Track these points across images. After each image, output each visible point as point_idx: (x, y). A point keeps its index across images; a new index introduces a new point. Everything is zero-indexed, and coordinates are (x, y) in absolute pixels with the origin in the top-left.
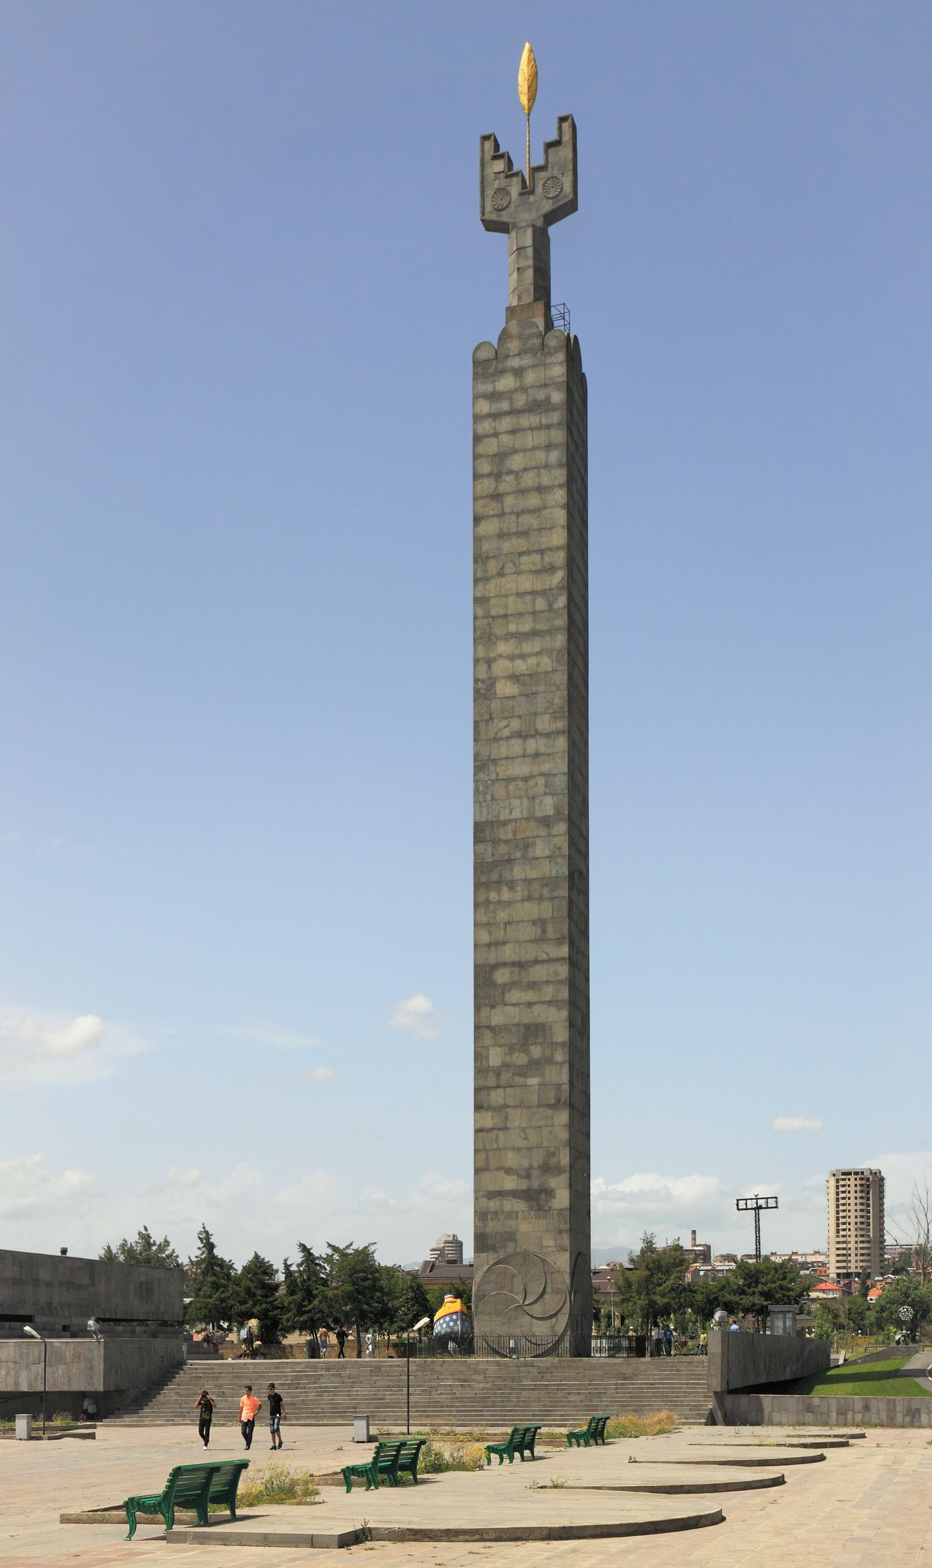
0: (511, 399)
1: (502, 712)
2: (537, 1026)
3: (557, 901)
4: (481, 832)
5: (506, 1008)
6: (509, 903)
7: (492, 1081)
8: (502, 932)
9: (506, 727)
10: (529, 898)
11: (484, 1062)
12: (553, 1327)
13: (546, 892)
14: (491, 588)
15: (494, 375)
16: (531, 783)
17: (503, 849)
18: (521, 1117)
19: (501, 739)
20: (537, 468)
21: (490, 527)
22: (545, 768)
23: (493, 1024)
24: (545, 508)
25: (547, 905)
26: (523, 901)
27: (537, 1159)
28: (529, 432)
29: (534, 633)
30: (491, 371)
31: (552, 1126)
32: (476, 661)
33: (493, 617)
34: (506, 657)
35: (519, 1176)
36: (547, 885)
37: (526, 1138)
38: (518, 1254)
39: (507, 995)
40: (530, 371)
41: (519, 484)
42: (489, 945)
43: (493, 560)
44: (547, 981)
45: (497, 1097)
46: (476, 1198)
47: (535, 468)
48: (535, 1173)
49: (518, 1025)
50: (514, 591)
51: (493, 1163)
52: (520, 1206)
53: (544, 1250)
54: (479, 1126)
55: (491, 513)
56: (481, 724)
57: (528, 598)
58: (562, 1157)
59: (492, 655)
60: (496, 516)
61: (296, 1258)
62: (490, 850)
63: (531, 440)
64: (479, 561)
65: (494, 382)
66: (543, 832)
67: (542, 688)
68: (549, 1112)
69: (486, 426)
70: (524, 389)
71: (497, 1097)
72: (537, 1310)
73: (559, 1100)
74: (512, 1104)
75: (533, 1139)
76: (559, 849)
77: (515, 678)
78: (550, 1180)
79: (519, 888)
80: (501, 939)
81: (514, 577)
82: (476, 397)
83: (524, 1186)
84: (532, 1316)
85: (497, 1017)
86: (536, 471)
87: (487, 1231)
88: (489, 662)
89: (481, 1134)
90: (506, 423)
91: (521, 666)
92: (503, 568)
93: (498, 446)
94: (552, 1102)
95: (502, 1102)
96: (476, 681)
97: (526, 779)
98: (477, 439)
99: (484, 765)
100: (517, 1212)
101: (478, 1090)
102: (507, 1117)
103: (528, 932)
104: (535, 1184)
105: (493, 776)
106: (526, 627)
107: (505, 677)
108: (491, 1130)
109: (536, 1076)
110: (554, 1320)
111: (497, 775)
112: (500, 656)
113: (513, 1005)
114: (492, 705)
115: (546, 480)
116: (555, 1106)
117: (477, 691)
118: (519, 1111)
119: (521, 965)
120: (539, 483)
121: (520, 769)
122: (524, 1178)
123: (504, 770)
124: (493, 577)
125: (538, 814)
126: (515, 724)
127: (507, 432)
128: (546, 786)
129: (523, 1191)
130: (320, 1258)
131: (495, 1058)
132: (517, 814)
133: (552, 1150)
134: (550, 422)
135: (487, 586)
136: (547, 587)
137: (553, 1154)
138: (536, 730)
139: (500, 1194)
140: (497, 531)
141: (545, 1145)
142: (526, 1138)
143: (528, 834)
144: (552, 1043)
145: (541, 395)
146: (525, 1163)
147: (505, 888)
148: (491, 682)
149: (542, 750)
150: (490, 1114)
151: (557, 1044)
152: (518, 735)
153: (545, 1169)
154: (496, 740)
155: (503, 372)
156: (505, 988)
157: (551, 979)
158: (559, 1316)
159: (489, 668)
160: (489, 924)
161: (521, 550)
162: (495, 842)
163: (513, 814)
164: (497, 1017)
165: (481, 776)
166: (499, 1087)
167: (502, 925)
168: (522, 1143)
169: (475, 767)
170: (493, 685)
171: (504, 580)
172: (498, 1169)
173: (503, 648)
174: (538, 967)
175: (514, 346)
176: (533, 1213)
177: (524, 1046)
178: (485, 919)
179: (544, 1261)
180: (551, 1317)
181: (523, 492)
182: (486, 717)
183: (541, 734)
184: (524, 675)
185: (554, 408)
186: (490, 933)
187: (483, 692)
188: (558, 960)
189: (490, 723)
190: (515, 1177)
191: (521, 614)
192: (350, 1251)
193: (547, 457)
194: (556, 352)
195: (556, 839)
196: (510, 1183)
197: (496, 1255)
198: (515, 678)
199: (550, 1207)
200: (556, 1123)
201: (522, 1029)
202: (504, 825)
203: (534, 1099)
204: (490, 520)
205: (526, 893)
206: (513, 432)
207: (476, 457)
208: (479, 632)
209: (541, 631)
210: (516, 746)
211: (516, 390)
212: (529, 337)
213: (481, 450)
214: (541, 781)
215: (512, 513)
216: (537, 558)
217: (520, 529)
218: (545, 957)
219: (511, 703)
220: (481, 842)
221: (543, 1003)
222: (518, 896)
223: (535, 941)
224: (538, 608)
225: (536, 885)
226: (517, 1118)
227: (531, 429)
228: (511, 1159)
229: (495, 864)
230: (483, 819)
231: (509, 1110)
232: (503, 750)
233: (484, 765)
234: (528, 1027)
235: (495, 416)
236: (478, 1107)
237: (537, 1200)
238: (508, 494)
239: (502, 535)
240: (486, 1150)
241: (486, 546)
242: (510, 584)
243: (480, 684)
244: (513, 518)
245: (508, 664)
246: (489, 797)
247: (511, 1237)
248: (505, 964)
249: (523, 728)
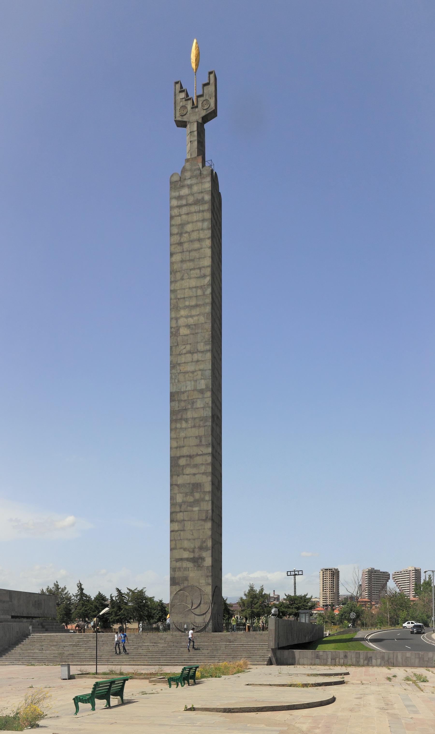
0: (187, 199)
1: (182, 342)
2: (197, 484)
3: (206, 428)
4: (173, 396)
5: (184, 476)
6: (186, 429)
7: (178, 509)
8: (182, 442)
9: (184, 349)
10: (194, 426)
11: (175, 501)
12: (204, 619)
13: (201, 423)
14: (178, 285)
15: (179, 188)
16: (195, 374)
17: (183, 404)
19: (182, 354)
20: (198, 230)
21: (177, 258)
22: (202, 367)
23: (178, 483)
24: (201, 248)
25: (202, 429)
26: (191, 427)
27: (197, 544)
28: (195, 214)
29: (197, 306)
30: (178, 186)
31: (204, 529)
32: (171, 319)
33: (179, 299)
34: (184, 317)
35: (190, 552)
36: (202, 420)
37: (193, 535)
38: (188, 586)
39: (184, 470)
40: (195, 186)
41: (190, 238)
42: (176, 448)
43: (178, 273)
44: (202, 464)
45: (180, 516)
46: (171, 562)
47: (197, 230)
48: (197, 550)
49: (189, 484)
50: (188, 287)
51: (178, 546)
52: (190, 565)
54: (172, 529)
55: (178, 251)
56: (173, 347)
57: (194, 290)
58: (208, 543)
59: (178, 316)
60: (180, 253)
61: (115, 594)
62: (177, 405)
63: (195, 217)
64: (173, 273)
65: (179, 191)
66: (200, 396)
67: (200, 331)
68: (203, 523)
69: (176, 212)
70: (192, 194)
71: (180, 516)
72: (197, 611)
73: (207, 517)
74: (186, 519)
76: (208, 404)
77: (188, 326)
79: (190, 422)
80: (182, 445)
81: (188, 280)
82: (171, 199)
83: (191, 556)
84: (195, 614)
85: (180, 480)
86: (198, 232)
88: (177, 319)
89: (173, 533)
90: (184, 210)
91: (191, 321)
92: (183, 276)
93: (181, 221)
94: (204, 518)
95: (182, 518)
96: (171, 328)
97: (193, 372)
98: (172, 218)
99: (175, 366)
100: (189, 568)
101: (171, 513)
102: (184, 526)
103: (194, 442)
104: (197, 555)
105: (179, 371)
106: (193, 303)
107: (183, 326)
109: (197, 507)
110: (205, 616)
111: (181, 370)
112: (182, 316)
113: (187, 475)
114: (178, 339)
115: (202, 236)
116: (205, 520)
117: (171, 333)
118: (189, 523)
119: (190, 457)
120: (199, 237)
121: (190, 368)
122: (192, 552)
123: (183, 368)
124: (178, 281)
125: (198, 388)
126: (188, 347)
127: (185, 214)
128: (202, 375)
129: (191, 558)
130: (124, 594)
131: (179, 499)
132: (189, 388)
133: (204, 540)
134: (204, 209)
135: (176, 285)
136: (202, 284)
137: (204, 542)
138: (197, 350)
139: (181, 560)
140: (181, 259)
141: (201, 537)
142: (193, 535)
143: (194, 397)
144: (204, 492)
145: (200, 197)
146: (192, 546)
147: (184, 422)
148: (178, 328)
149: (200, 358)
150: (177, 524)
151: (207, 492)
152: (190, 352)
153: (201, 548)
154: (180, 354)
155: (183, 187)
156: (184, 467)
157: (203, 463)
158: (207, 614)
159: (177, 322)
160: (177, 438)
161: (191, 268)
162: (179, 401)
163: (188, 388)
164: (180, 480)
165: (173, 371)
166: (181, 512)
167: (182, 439)
168: (190, 537)
169: (171, 367)
170: (178, 330)
171: (183, 282)
172: (181, 548)
173: (183, 313)
174: (198, 457)
175: (188, 174)
176: (196, 568)
177: (192, 493)
178: (175, 436)
179: (200, 589)
180: (204, 614)
181: (192, 241)
182: (176, 344)
183: (200, 352)
184: (192, 325)
185: (206, 203)
186: (177, 442)
187: (174, 333)
188: (207, 454)
189: (177, 347)
190: (188, 552)
191: (190, 297)
192: (136, 591)
193: (202, 225)
194: (206, 176)
195: (206, 400)
196: (186, 555)
198: (188, 326)
199: (203, 565)
200: (206, 528)
201: (191, 485)
202: (183, 393)
203: (196, 517)
204: (178, 254)
205: (193, 424)
206: (188, 214)
207: (171, 226)
208: (172, 306)
209: (200, 305)
210: (189, 357)
211: (189, 195)
212: (195, 170)
213: (173, 222)
214: (199, 373)
215: (187, 251)
216: (198, 271)
217: (191, 258)
218: (201, 453)
219: (186, 338)
220: (173, 401)
221: (200, 473)
222: (189, 425)
223: (197, 446)
224: (198, 294)
225: (197, 420)
226: (189, 526)
227: (195, 212)
228: (186, 544)
229: (179, 411)
230: (174, 391)
231: (185, 522)
232: (183, 359)
233: (175, 366)
234: (193, 484)
235: (180, 207)
236: (172, 521)
237: (197, 562)
238: (185, 242)
239: (182, 261)
240: (175, 540)
241: (175, 267)
242: (185, 283)
243: (173, 330)
244: (188, 253)
245: (185, 320)
246: (176, 381)
247: (186, 579)
248: (183, 456)
249: (192, 349)
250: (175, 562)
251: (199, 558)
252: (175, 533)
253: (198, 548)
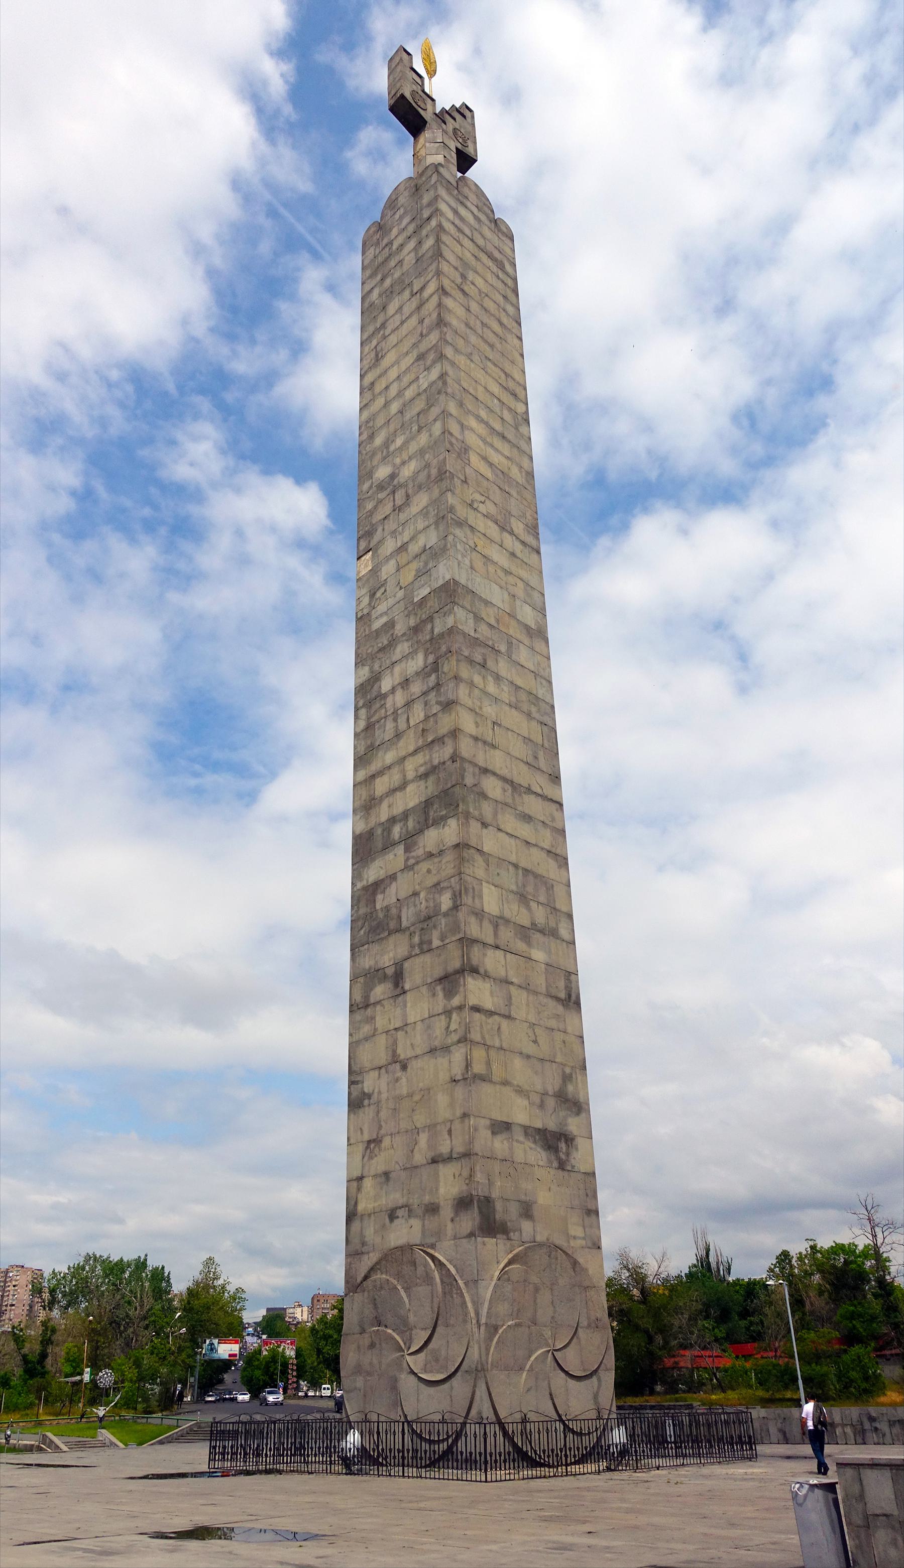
18: (528, 1005)
53: (572, 1243)
66: (527, 641)
84: (567, 1373)
106: (497, 426)
108: (491, 1013)
110: (594, 1379)
129: (538, 1131)
142: (535, 1042)
150: (488, 985)
158: (601, 1372)
168: (530, 1049)
172: (505, 1083)
179: (575, 1263)
180: (590, 1376)
218: (539, 791)
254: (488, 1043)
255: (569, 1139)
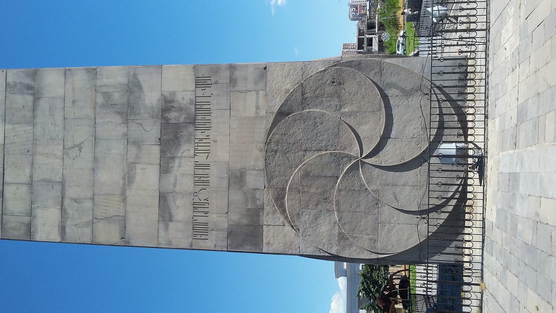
27: (111, 126)
37: (80, 147)
38: (266, 165)
51: (114, 208)
68: (43, 104)
73: (29, 87)
74: (28, 171)
75: (82, 133)
78: (147, 102)
87: (226, 226)
94: (30, 98)
95: (24, 189)
100: (197, 166)
102: (48, 181)
104: (152, 131)
108: (63, 210)
110: (390, 92)
116: (34, 91)
118: (39, 159)
129: (163, 152)
133: (100, 99)
137: (107, 96)
139: (163, 198)
142: (80, 147)
146: (118, 148)
150: (39, 213)
153: (128, 111)
180: (385, 97)
196: (148, 177)
197: (267, 209)
203: (23, 130)
226: (49, 165)
228: (110, 176)
231: (35, 178)
237: (178, 127)
250: (171, 225)
251: (163, 118)
252: (69, 222)
253: (126, 122)
254: (90, 218)
255: (168, 105)
